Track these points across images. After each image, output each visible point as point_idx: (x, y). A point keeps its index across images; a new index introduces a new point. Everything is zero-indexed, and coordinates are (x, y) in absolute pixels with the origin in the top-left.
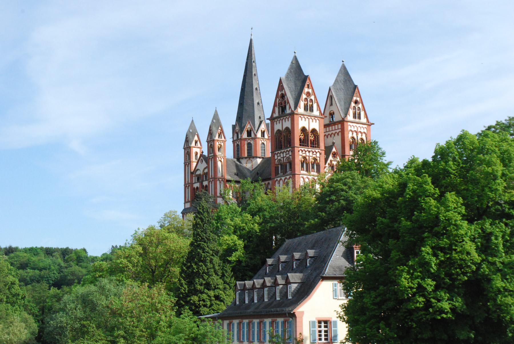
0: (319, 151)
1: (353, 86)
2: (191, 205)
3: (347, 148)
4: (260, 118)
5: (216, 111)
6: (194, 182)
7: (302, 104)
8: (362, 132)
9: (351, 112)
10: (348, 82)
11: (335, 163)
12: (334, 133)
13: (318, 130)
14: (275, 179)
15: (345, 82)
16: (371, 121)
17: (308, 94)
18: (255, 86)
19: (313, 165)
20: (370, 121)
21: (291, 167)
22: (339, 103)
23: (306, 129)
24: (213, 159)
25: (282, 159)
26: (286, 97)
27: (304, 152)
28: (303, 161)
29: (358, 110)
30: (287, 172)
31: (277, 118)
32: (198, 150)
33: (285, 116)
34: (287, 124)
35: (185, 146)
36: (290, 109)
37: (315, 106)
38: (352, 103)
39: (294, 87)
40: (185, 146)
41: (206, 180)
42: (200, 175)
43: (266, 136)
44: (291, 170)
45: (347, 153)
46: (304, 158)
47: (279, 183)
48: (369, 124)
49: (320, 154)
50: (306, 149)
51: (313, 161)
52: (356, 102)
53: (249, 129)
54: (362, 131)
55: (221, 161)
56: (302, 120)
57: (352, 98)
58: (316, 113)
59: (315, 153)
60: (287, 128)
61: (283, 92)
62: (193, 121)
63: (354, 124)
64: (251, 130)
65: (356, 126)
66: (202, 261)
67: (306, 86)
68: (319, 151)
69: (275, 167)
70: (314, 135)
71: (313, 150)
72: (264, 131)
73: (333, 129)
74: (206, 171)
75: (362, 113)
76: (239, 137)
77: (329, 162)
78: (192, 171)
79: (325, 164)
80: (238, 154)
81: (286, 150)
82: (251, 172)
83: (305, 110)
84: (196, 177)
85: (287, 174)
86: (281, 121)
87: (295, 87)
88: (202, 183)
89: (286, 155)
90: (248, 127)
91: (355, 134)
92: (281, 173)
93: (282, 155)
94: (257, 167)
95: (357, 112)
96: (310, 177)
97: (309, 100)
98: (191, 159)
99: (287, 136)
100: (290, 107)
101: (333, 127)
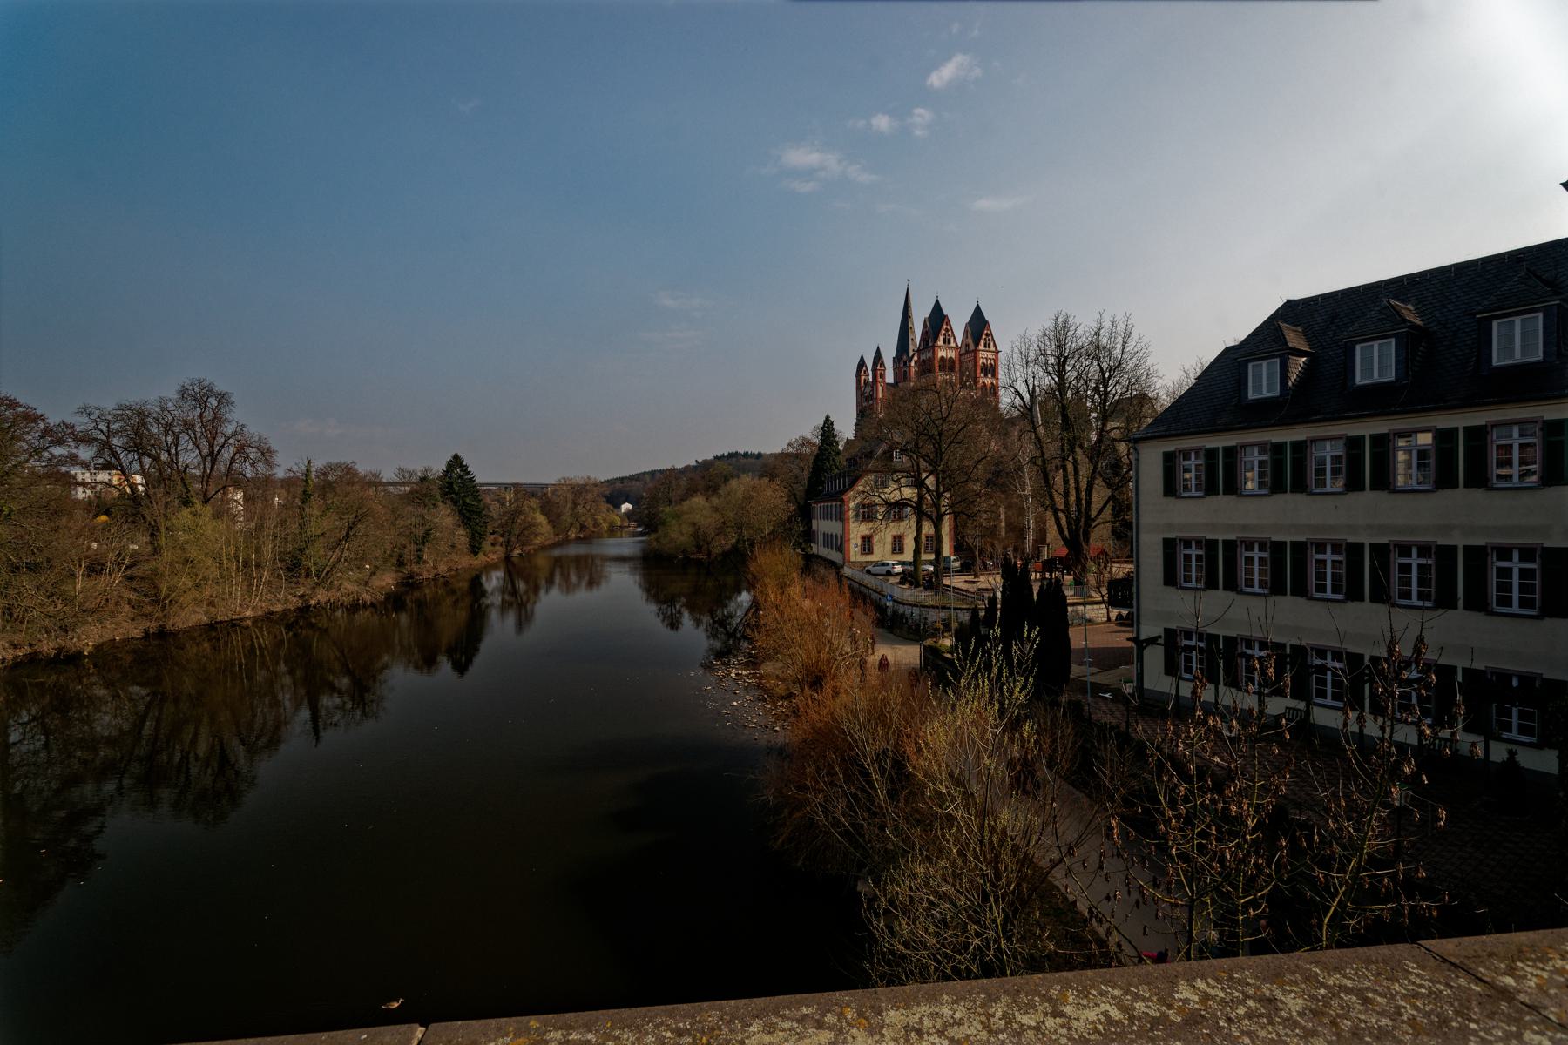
3: (978, 371)
7: (941, 338)
9: (982, 342)
13: (954, 357)
16: (999, 349)
18: (910, 325)
34: (929, 354)
52: (987, 335)
54: (991, 357)
75: (992, 344)
90: (905, 357)
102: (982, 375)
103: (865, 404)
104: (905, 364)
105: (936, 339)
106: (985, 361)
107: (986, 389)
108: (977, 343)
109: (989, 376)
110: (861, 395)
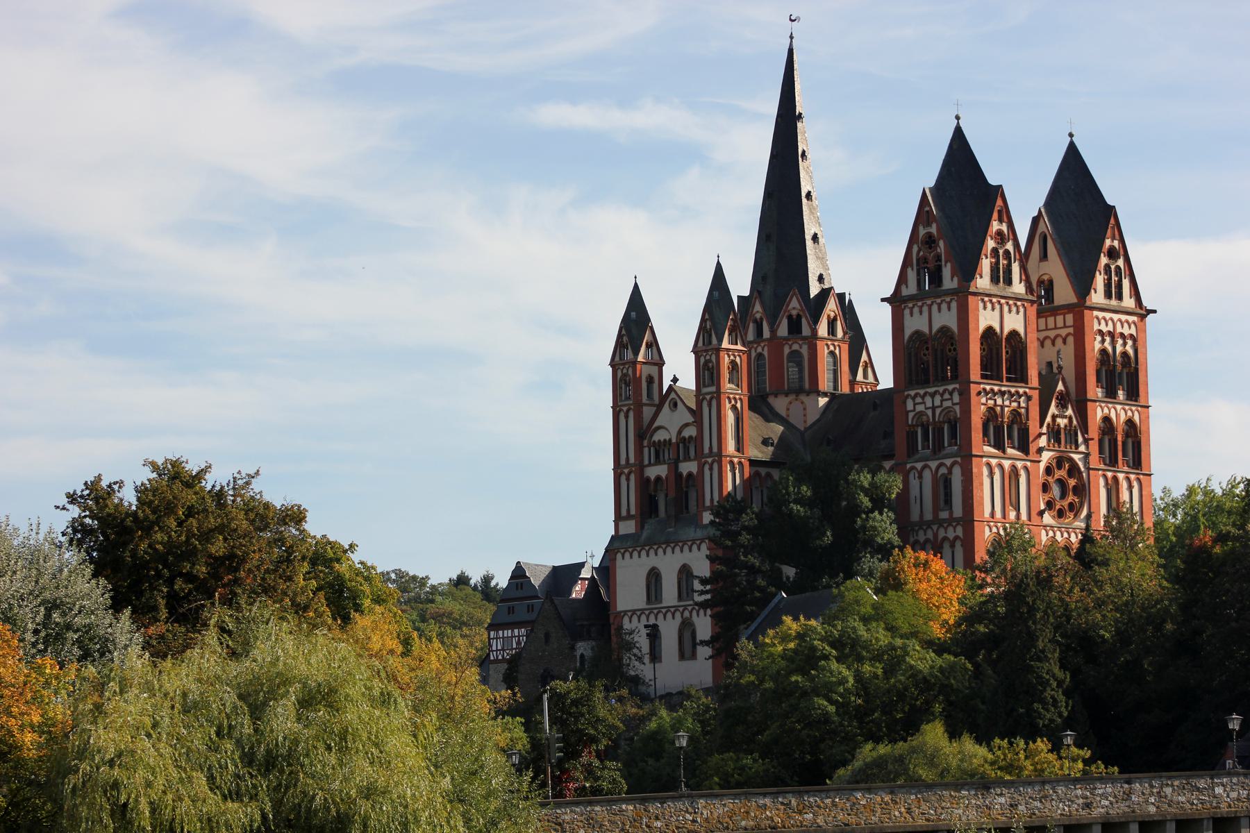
0: (1027, 390)
2: (641, 526)
4: (821, 279)
5: (719, 269)
6: (646, 462)
7: (986, 264)
9: (1100, 280)
11: (1062, 422)
13: (1021, 331)
14: (908, 466)
17: (1000, 233)
19: (1010, 428)
20: (1145, 303)
21: (953, 435)
24: (714, 403)
29: (1116, 275)
30: (944, 447)
31: (911, 298)
32: (653, 370)
33: (940, 297)
34: (946, 318)
37: (1016, 268)
38: (1102, 255)
41: (687, 458)
42: (668, 443)
43: (840, 334)
44: (956, 444)
45: (1090, 395)
46: (991, 410)
47: (920, 477)
48: (1143, 313)
49: (1029, 398)
50: (996, 388)
52: (1112, 254)
53: (794, 313)
54: (1126, 331)
55: (734, 408)
56: (985, 308)
58: (1018, 288)
60: (944, 330)
61: (933, 229)
62: (636, 286)
63: (1108, 315)
64: (799, 316)
65: (1112, 319)
67: (995, 215)
68: (1027, 390)
69: (908, 433)
70: (1012, 347)
71: (1013, 390)
72: (835, 319)
73: (1051, 325)
74: (691, 432)
75: (1126, 283)
76: (766, 333)
77: (1049, 419)
79: (1041, 426)
81: (941, 389)
82: (802, 434)
83: (992, 281)
86: (925, 309)
88: (677, 467)
89: (942, 401)
90: (794, 305)
91: (1108, 339)
92: (923, 449)
93: (928, 400)
94: (818, 420)
95: (1114, 278)
97: (1001, 252)
101: (1051, 320)
102: (1100, 392)
103: (653, 472)
104: (795, 326)
105: (968, 271)
106: (1107, 345)
107: (1114, 442)
108: (1083, 286)
109: (1121, 394)
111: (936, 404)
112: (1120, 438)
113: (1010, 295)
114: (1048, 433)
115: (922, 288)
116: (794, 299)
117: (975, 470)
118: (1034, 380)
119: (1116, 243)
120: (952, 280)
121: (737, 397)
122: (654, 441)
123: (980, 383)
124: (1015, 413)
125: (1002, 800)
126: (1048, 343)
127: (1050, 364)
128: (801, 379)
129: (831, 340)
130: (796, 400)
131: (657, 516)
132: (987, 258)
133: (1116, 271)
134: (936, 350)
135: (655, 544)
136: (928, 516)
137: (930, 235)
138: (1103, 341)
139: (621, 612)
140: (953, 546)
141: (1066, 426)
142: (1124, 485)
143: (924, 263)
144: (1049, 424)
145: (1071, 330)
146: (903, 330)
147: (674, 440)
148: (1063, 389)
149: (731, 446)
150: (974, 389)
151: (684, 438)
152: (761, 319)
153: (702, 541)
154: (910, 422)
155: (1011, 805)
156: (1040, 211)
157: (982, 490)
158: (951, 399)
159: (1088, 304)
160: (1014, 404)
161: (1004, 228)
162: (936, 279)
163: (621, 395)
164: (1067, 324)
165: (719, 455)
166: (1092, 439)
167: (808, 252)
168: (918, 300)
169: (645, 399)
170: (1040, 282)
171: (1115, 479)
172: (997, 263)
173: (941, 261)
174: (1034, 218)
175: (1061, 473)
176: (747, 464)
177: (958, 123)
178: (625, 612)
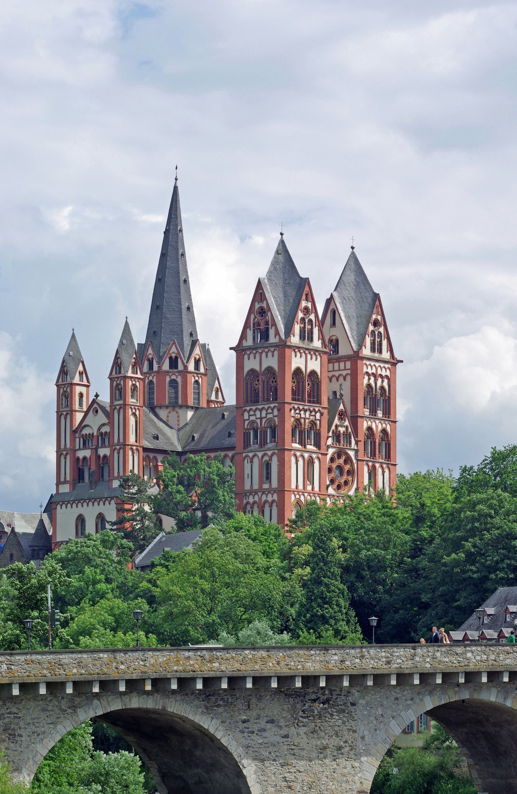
1: (369, 295)
3: (361, 403)
4: (191, 335)
6: (77, 447)
7: (297, 328)
8: (383, 375)
9: (368, 340)
10: (362, 286)
12: (337, 375)
13: (318, 371)
14: (244, 454)
15: (357, 285)
16: (398, 356)
21: (273, 435)
22: (349, 322)
23: (302, 372)
24: (122, 411)
25: (258, 421)
26: (269, 314)
27: (298, 411)
28: (296, 427)
30: (267, 443)
31: (250, 348)
32: (83, 390)
33: (267, 347)
35: (60, 380)
36: (277, 337)
37: (316, 331)
38: (370, 324)
39: (281, 296)
40: (60, 380)
41: (103, 446)
44: (275, 442)
46: (298, 420)
47: (252, 462)
48: (394, 362)
49: (322, 414)
51: (310, 425)
52: (376, 324)
53: (173, 355)
54: (384, 373)
55: (134, 414)
56: (296, 356)
57: (371, 316)
58: (317, 344)
59: (313, 413)
60: (269, 369)
61: (264, 305)
62: (73, 334)
64: (176, 358)
66: (326, 603)
67: (304, 297)
69: (244, 433)
70: (312, 381)
73: (336, 368)
74: (106, 429)
75: (385, 343)
76: (155, 368)
77: (333, 427)
78: (74, 428)
79: (328, 432)
80: (151, 399)
81: (266, 407)
83: (300, 338)
84: (81, 439)
85: (267, 447)
86: (258, 355)
87: (285, 297)
88: (97, 452)
89: (266, 414)
90: (174, 349)
91: (372, 379)
92: (254, 444)
93: (258, 413)
95: (377, 340)
96: (306, 455)
97: (307, 320)
98: (73, 407)
99: (268, 382)
100: (277, 333)
101: (336, 365)
102: (367, 412)
103: (81, 454)
104: (174, 363)
106: (372, 381)
107: (373, 443)
109: (380, 414)
110: (74, 432)
111: (262, 416)
112: (377, 441)
113: (311, 348)
114: (333, 437)
115: (256, 342)
116: (174, 346)
117: (286, 458)
118: (325, 404)
119: (379, 317)
120: (275, 337)
121: (136, 407)
122: (83, 435)
123: (290, 404)
124: (313, 423)
125: (336, 658)
126: (334, 379)
127: (335, 393)
128: (177, 398)
129: (196, 373)
130: (173, 411)
131: (84, 482)
132: (298, 324)
133: (378, 335)
134: (264, 381)
135: (82, 500)
136: (256, 487)
137: (262, 308)
138: (369, 379)
139: (58, 542)
140: (271, 506)
141: (344, 432)
142: (380, 471)
143: (258, 326)
144: (333, 431)
145: (349, 372)
146: (243, 368)
147: (95, 434)
148: (343, 409)
149: (132, 439)
150: (287, 407)
151: (102, 433)
152: (152, 358)
153: (112, 498)
154: (246, 427)
155: (342, 661)
156: (332, 295)
157: (290, 471)
158: (272, 413)
159: (360, 355)
160: (311, 417)
161: (309, 305)
162: (265, 336)
163: (62, 404)
164: (347, 368)
165: (124, 445)
166: (360, 441)
167: (183, 316)
168: (253, 349)
169: (77, 407)
170: (331, 341)
171: (374, 467)
172: (304, 327)
173: (268, 325)
174: (327, 300)
175: (341, 461)
176: (141, 450)
177: (282, 237)
178: (62, 542)
